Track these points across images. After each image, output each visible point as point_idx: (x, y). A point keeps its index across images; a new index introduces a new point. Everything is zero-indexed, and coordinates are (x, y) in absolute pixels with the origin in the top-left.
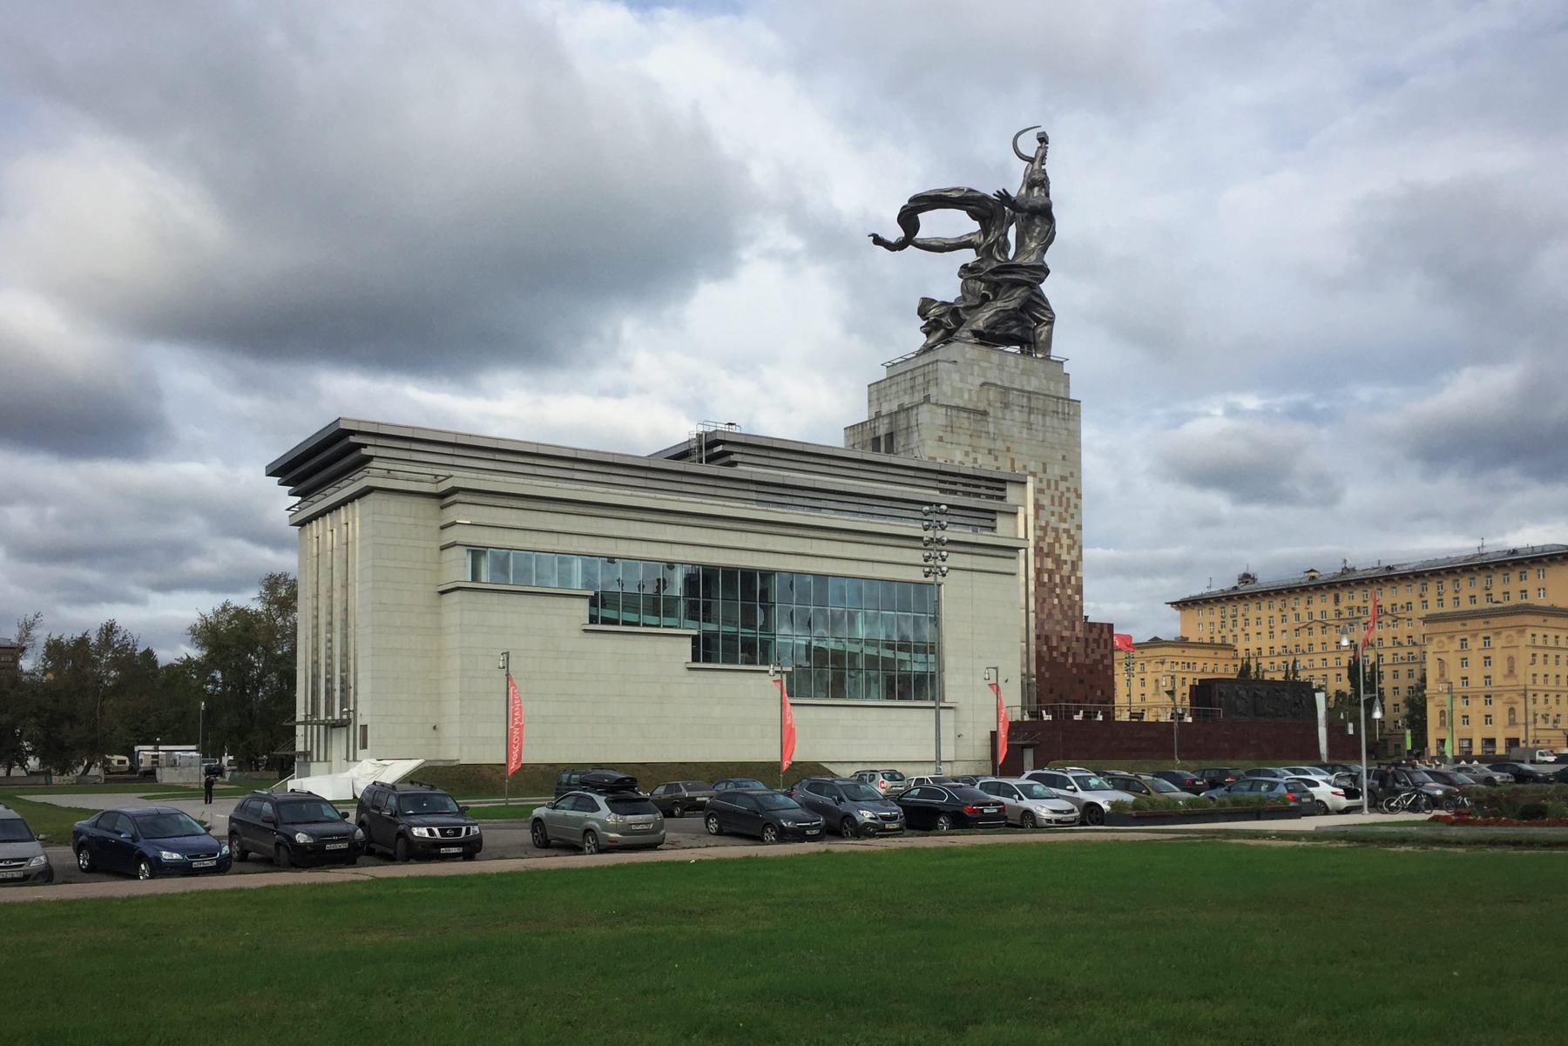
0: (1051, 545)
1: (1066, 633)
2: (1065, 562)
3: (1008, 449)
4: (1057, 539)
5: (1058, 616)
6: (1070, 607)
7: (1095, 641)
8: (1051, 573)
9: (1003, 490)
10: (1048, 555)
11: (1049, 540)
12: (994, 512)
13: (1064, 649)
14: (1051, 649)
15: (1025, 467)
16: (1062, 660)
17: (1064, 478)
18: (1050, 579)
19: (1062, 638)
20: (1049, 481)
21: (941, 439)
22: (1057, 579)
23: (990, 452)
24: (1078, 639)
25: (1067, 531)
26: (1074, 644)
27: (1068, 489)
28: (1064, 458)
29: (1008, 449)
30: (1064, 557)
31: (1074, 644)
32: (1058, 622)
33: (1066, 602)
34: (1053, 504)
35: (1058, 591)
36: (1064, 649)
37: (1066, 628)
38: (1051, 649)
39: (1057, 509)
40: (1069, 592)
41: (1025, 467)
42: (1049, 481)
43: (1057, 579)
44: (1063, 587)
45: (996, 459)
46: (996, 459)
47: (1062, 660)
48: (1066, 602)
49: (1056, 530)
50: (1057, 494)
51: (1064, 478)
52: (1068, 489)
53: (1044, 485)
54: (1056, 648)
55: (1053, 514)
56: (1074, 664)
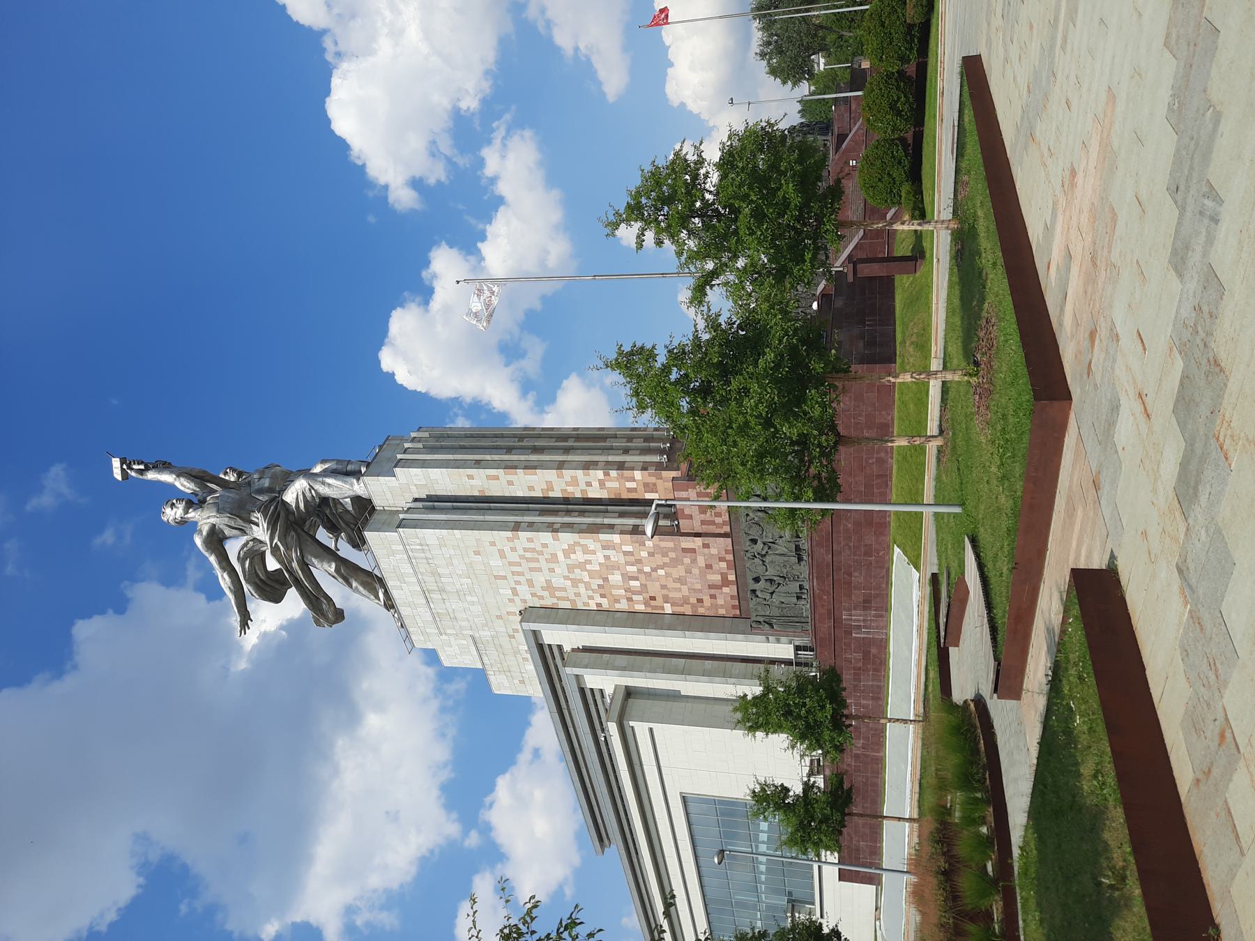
0: (592, 574)
1: (701, 561)
2: (607, 558)
3: (499, 617)
4: (582, 566)
5: (679, 571)
6: (665, 555)
8: (628, 577)
10: (606, 579)
12: (582, 691)
14: (725, 582)
15: (511, 601)
18: (636, 579)
19: (709, 567)
20: (513, 573)
22: (632, 569)
24: (706, 546)
25: (567, 554)
26: (714, 551)
27: (513, 549)
28: (477, 553)
29: (499, 617)
30: (600, 557)
32: (688, 571)
33: (659, 559)
34: (540, 570)
35: (647, 569)
37: (694, 561)
38: (725, 582)
40: (644, 554)
41: (511, 601)
43: (632, 569)
44: (639, 561)
48: (659, 559)
49: (571, 568)
51: (502, 554)
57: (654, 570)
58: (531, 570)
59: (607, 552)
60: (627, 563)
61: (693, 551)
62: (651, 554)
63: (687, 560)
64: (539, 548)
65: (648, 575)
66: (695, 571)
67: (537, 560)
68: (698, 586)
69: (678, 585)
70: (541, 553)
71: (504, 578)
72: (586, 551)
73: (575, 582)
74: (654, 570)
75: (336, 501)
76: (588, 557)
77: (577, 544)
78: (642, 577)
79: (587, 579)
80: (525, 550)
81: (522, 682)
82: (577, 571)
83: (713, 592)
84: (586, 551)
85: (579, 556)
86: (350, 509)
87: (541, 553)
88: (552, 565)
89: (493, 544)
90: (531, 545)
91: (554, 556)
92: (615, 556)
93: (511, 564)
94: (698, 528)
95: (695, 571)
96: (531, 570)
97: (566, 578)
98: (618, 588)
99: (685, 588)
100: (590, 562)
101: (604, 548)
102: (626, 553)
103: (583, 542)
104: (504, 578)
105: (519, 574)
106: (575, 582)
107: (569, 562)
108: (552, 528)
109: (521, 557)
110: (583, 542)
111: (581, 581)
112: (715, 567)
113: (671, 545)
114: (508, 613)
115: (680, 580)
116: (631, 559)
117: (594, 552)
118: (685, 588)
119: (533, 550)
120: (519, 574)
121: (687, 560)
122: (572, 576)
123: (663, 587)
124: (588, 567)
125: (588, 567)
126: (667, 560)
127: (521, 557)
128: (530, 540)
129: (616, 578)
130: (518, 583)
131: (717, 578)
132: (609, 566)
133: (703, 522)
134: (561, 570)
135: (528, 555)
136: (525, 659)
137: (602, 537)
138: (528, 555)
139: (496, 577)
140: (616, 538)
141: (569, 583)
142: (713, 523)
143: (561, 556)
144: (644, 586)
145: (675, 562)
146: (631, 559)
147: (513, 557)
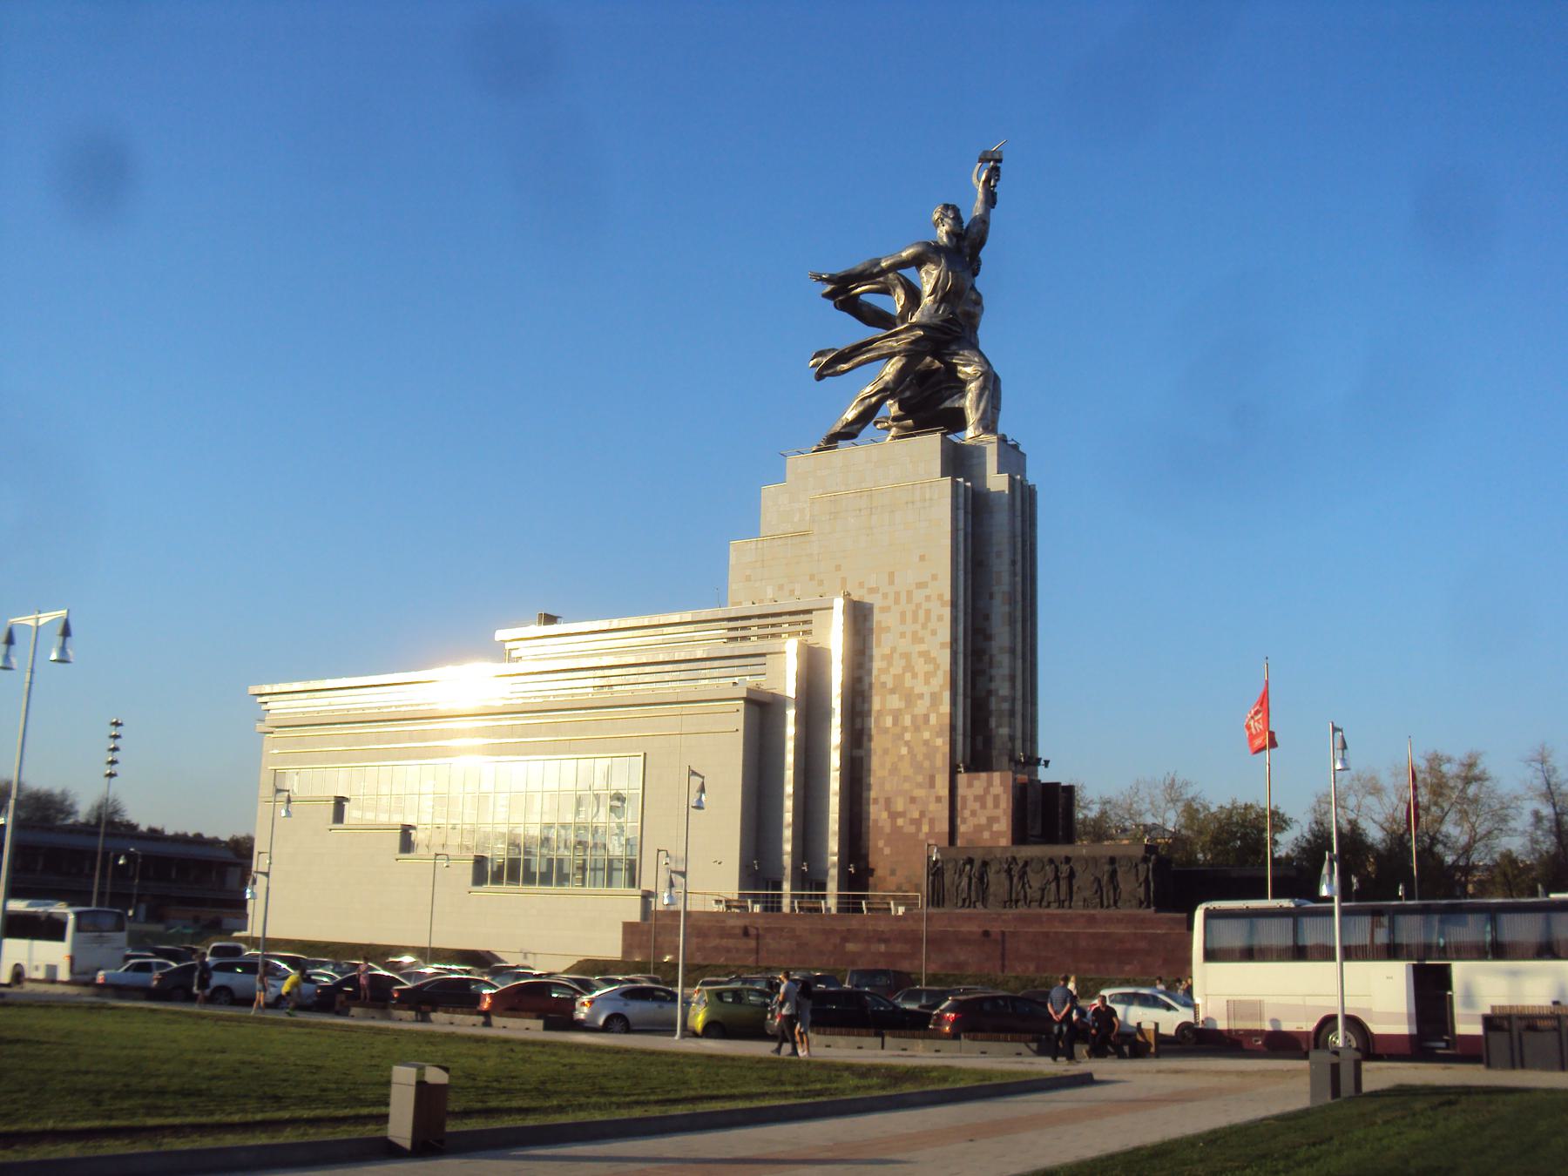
0: (899, 678)
1: (920, 793)
2: (921, 696)
3: (838, 568)
4: (909, 667)
5: (906, 769)
6: (927, 756)
7: (976, 798)
10: (893, 691)
11: (896, 669)
13: (916, 815)
14: (894, 816)
15: (861, 585)
16: (912, 829)
18: (895, 722)
19: (913, 800)
20: (897, 594)
23: (812, 578)
24: (938, 799)
26: (932, 807)
27: (928, 598)
28: (922, 558)
29: (838, 568)
30: (920, 688)
31: (932, 807)
32: (906, 779)
33: (920, 751)
35: (908, 736)
36: (916, 815)
37: (919, 786)
38: (894, 816)
40: (926, 735)
41: (861, 585)
42: (897, 594)
43: (907, 720)
44: (917, 729)
45: (821, 583)
47: (912, 829)
49: (906, 656)
52: (928, 598)
54: (902, 814)
55: (903, 635)
57: (907, 744)
58: (903, 614)
59: (927, 698)
60: (914, 718)
61: (932, 784)
62: (926, 743)
63: (920, 779)
64: (931, 625)
65: (900, 737)
67: (915, 620)
68: (888, 787)
69: (888, 766)
70: (924, 626)
71: (891, 582)
72: (928, 677)
73: (888, 658)
74: (907, 744)
75: (964, 396)
76: (921, 678)
77: (937, 667)
78: (898, 730)
79: (893, 671)
80: (928, 612)
81: (748, 578)
82: (903, 662)
83: (882, 801)
84: (928, 677)
85: (921, 666)
86: (948, 404)
87: (924, 626)
88: (909, 636)
89: (934, 577)
90: (934, 617)
91: (922, 641)
92: (921, 707)
93: (909, 593)
94: (962, 790)
95: (907, 786)
96: (903, 614)
97: (894, 650)
98: (883, 702)
100: (915, 676)
102: (926, 718)
104: (891, 582)
105: (897, 601)
106: (888, 658)
108: (954, 640)
109: (919, 606)
111: (890, 664)
112: (913, 807)
114: (844, 580)
115: (894, 770)
117: (927, 682)
118: (886, 773)
119: (928, 618)
120: (897, 601)
121: (920, 779)
122: (896, 656)
123: (886, 751)
124: (908, 676)
125: (908, 676)
126: (920, 757)
127: (919, 606)
128: (940, 618)
129: (895, 702)
130: (885, 596)
131: (899, 805)
132: (910, 698)
134: (904, 645)
135: (921, 613)
137: (946, 695)
138: (921, 613)
139: (891, 575)
140: (945, 708)
141: (887, 651)
143: (923, 647)
144: (886, 731)
145: (918, 767)
147: (919, 596)
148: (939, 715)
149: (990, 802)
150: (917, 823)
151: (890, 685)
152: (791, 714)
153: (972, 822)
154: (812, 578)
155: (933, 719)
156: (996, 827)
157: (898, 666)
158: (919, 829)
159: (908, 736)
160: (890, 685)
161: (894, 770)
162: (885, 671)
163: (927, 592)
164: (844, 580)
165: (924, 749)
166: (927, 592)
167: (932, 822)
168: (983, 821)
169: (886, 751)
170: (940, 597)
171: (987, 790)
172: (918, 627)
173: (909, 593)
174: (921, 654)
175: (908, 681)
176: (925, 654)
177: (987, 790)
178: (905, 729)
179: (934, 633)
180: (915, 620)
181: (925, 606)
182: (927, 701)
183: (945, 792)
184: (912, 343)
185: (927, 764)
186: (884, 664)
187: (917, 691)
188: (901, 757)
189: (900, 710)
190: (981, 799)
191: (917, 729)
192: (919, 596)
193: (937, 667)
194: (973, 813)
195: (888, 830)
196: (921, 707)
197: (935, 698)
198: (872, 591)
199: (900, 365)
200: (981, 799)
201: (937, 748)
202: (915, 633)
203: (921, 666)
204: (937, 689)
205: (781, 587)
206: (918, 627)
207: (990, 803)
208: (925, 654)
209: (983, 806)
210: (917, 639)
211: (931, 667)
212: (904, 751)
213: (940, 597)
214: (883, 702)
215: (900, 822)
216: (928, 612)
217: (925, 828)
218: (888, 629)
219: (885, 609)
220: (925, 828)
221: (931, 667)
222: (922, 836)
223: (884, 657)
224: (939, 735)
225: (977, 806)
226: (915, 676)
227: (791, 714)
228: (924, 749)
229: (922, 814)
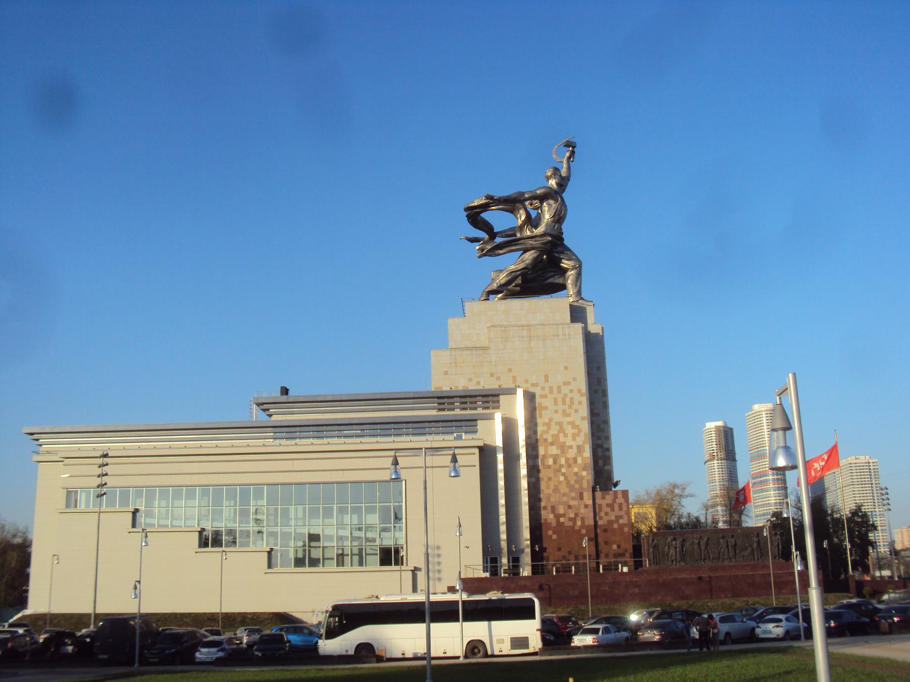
0: (556, 437)
1: (572, 503)
2: (571, 447)
4: (562, 430)
5: (564, 489)
6: (577, 482)
7: (608, 505)
9: (498, 402)
10: (552, 444)
11: (554, 430)
14: (558, 517)
16: (570, 524)
17: (566, 383)
18: (555, 462)
19: (570, 507)
21: (446, 373)
22: (563, 461)
23: (492, 375)
24: (586, 506)
26: (582, 510)
27: (571, 391)
28: (566, 368)
29: (510, 370)
30: (570, 442)
31: (582, 510)
32: (564, 495)
35: (563, 470)
36: (572, 515)
37: (573, 499)
38: (558, 517)
39: (560, 407)
40: (576, 470)
43: (563, 461)
44: (569, 466)
45: (498, 379)
46: (498, 379)
49: (560, 424)
50: (561, 396)
51: (566, 383)
52: (571, 391)
53: (547, 391)
54: (564, 515)
55: (556, 412)
56: (583, 526)
57: (563, 474)
58: (556, 400)
60: (567, 460)
62: (576, 474)
63: (573, 494)
64: (575, 407)
65: (559, 470)
66: (565, 499)
67: (564, 403)
68: (552, 499)
69: (552, 487)
70: (570, 407)
71: (547, 380)
72: (574, 437)
73: (548, 425)
74: (563, 474)
76: (570, 436)
77: (580, 431)
78: (557, 466)
79: (551, 432)
80: (572, 399)
82: (558, 427)
83: (549, 508)
84: (574, 437)
85: (569, 430)
87: (570, 407)
88: (560, 412)
90: (576, 402)
91: (569, 415)
92: (571, 453)
93: (559, 388)
94: (598, 501)
95: (565, 499)
97: (551, 420)
98: (546, 451)
99: (550, 491)
100: (566, 435)
101: (579, 447)
102: (575, 460)
103: (582, 435)
104: (547, 380)
105: (551, 391)
106: (548, 425)
107: (565, 425)
110: (582, 435)
111: (549, 428)
113: (585, 485)
114: (514, 378)
115: (556, 490)
116: (571, 462)
117: (574, 439)
118: (550, 491)
120: (551, 391)
122: (553, 424)
123: (550, 479)
124: (561, 435)
125: (561, 435)
126: (572, 482)
127: (565, 395)
129: (554, 450)
130: (543, 388)
131: (561, 510)
132: (563, 448)
133: (600, 506)
134: (558, 417)
135: (568, 400)
136: (470, 380)
141: (547, 421)
142: (600, 510)
144: (549, 467)
145: (572, 488)
146: (571, 462)
147: (565, 390)
148: (583, 459)
149: (616, 507)
150: (573, 520)
151: (550, 440)
152: (500, 457)
153: (606, 519)
154: (492, 375)
155: (579, 460)
156: (621, 521)
157: (554, 430)
158: (575, 523)
159: (563, 470)
160: (550, 440)
161: (556, 490)
162: (547, 432)
163: (571, 387)
164: (514, 378)
165: (575, 478)
166: (571, 387)
167: (583, 519)
168: (613, 518)
169: (550, 479)
170: (579, 391)
171: (614, 501)
172: (566, 407)
173: (559, 388)
174: (569, 423)
175: (562, 439)
176: (572, 424)
177: (614, 501)
178: (562, 466)
179: (576, 411)
180: (564, 403)
181: (570, 395)
182: (575, 450)
183: (590, 502)
184: (544, 244)
185: (577, 486)
186: (545, 428)
187: (568, 444)
188: (561, 482)
189: (557, 455)
190: (611, 506)
191: (569, 466)
192: (565, 390)
193: (580, 431)
194: (607, 514)
195: (554, 524)
196: (571, 453)
197: (580, 449)
198: (533, 385)
199: (535, 255)
200: (611, 506)
201: (583, 477)
202: (564, 411)
203: (569, 430)
204: (580, 443)
205: (470, 380)
206: (566, 407)
207: (616, 507)
208: (572, 424)
209: (613, 510)
210: (565, 414)
211: (576, 431)
212: (562, 478)
213: (579, 391)
214: (546, 451)
215: (562, 520)
216: (572, 399)
217: (579, 523)
218: (546, 408)
219: (545, 396)
220: (579, 523)
221: (576, 431)
222: (577, 528)
223: (544, 424)
224: (584, 469)
225: (608, 510)
226: (566, 435)
227: (500, 457)
228: (575, 478)
229: (576, 515)
